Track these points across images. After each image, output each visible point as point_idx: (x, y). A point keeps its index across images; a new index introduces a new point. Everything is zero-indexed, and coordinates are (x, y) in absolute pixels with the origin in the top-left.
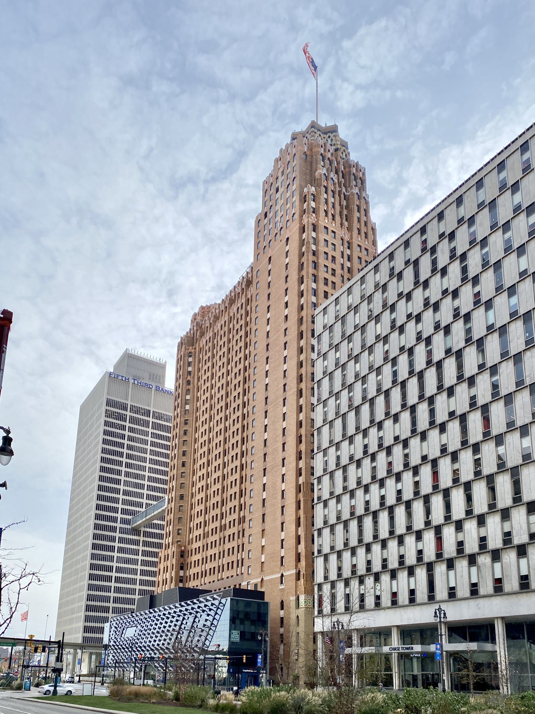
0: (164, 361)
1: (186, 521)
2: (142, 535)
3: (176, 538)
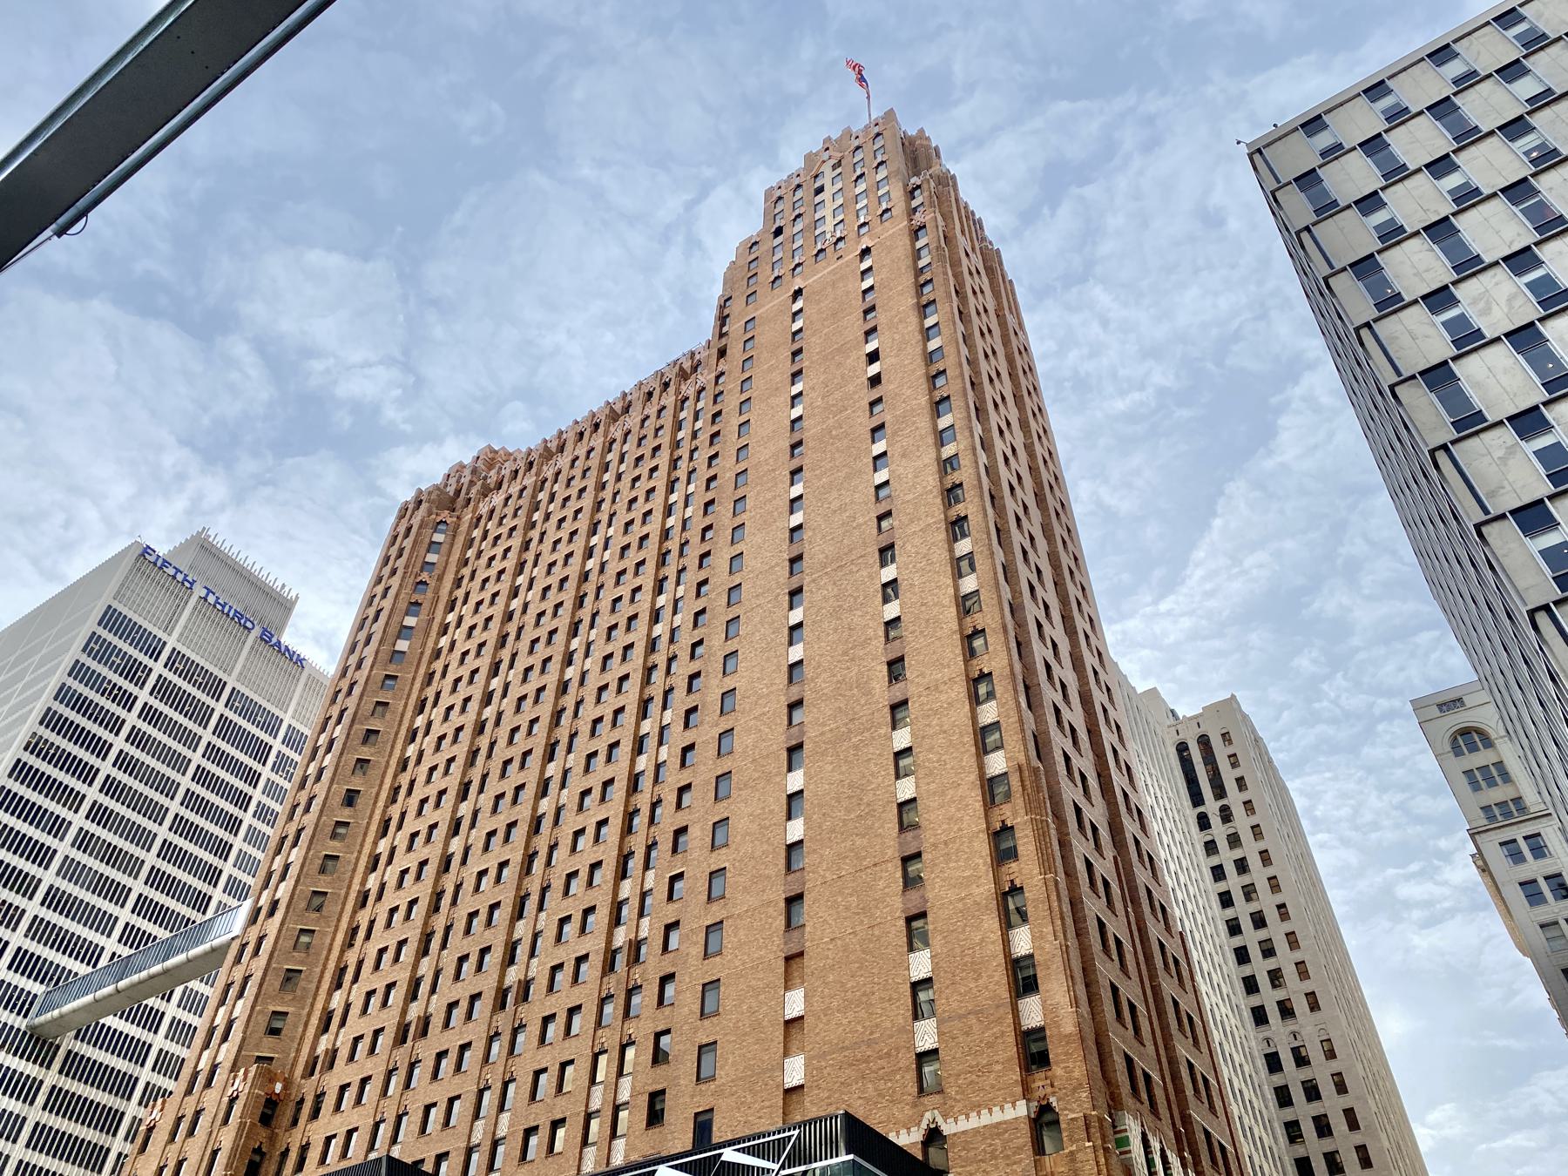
0: (293, 594)
1: (313, 986)
2: (56, 1065)
3: (257, 1047)
